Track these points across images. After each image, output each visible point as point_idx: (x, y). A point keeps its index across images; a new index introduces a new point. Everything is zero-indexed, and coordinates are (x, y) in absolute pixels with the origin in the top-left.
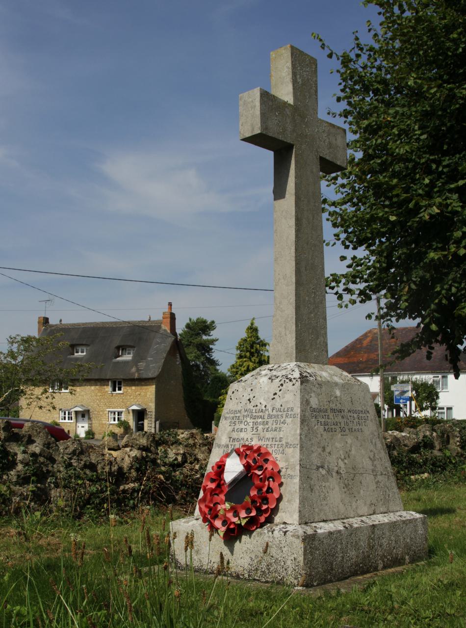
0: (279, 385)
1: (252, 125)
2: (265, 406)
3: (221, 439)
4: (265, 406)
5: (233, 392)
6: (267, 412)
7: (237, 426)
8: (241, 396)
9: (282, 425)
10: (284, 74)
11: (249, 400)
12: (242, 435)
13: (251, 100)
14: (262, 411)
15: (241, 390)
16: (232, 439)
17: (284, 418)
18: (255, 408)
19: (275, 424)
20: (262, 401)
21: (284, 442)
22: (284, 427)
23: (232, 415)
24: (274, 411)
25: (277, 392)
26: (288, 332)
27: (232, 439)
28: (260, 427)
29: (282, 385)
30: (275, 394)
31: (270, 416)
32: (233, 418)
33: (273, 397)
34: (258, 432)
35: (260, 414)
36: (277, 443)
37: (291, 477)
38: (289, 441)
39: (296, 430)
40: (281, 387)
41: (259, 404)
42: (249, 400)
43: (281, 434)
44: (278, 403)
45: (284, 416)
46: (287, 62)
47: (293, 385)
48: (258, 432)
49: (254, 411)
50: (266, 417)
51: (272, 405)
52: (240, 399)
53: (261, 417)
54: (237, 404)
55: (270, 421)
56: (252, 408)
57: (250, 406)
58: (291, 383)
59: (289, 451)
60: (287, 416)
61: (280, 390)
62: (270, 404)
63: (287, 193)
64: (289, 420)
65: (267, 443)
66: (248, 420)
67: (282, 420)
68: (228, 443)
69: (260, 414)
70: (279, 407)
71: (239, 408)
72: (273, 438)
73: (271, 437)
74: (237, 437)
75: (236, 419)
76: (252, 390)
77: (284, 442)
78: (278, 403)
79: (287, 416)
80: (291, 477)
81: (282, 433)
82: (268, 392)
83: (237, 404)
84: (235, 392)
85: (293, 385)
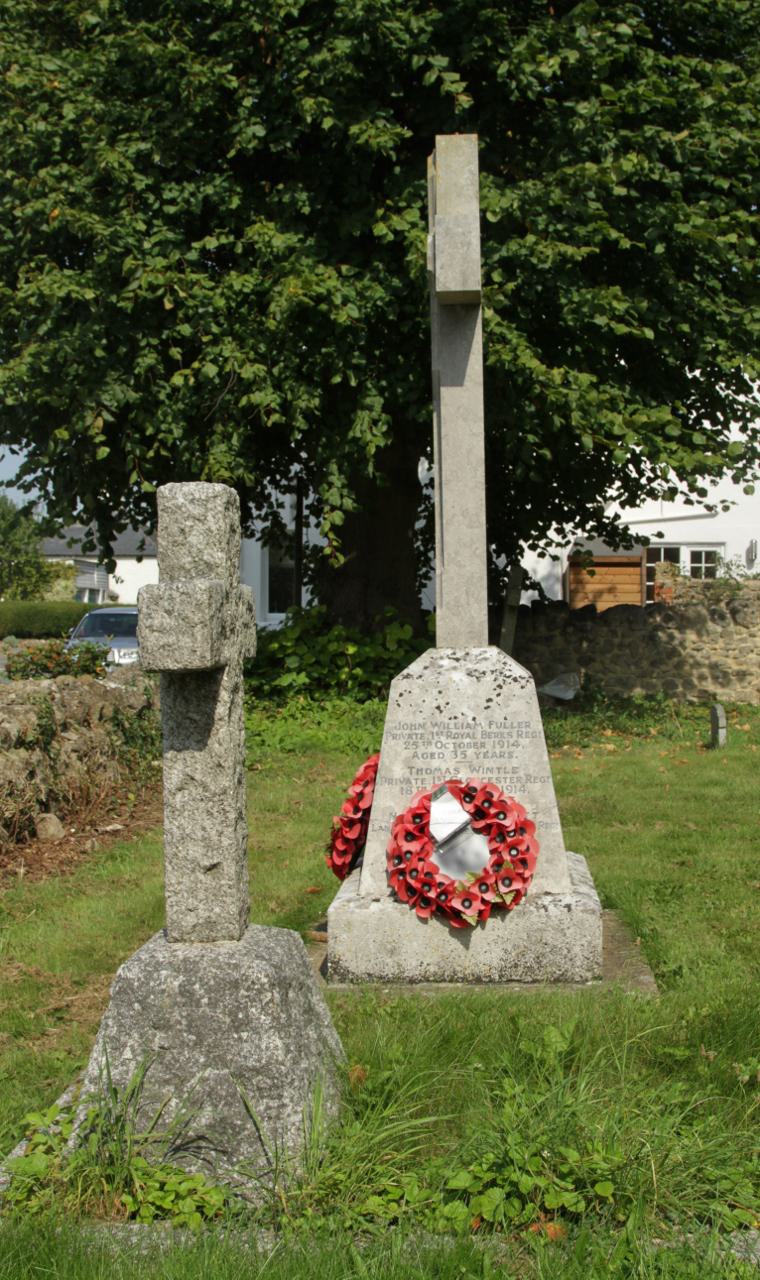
0: (494, 686)
1: (463, 273)
2: (474, 719)
3: (391, 771)
4: (474, 719)
5: (401, 695)
6: (479, 728)
7: (421, 750)
8: (420, 702)
9: (512, 749)
10: (463, 182)
11: (438, 708)
12: (435, 763)
13: (460, 230)
14: (468, 726)
15: (416, 691)
16: (414, 770)
17: (515, 738)
18: (453, 721)
19: (498, 746)
20: (465, 710)
21: (521, 774)
22: (517, 751)
23: (408, 732)
24: (493, 727)
25: (493, 697)
26: (472, 600)
27: (414, 770)
28: (470, 752)
29: (500, 687)
30: (489, 700)
31: (485, 734)
32: (410, 736)
33: (486, 705)
34: (468, 759)
35: (467, 731)
36: (508, 776)
37: (547, 825)
38: (531, 772)
39: (541, 756)
40: (498, 691)
41: (459, 715)
42: (438, 708)
43: (515, 763)
44: (498, 714)
45: (515, 735)
46: (470, 163)
47: (522, 687)
48: (468, 759)
49: (452, 726)
50: (479, 736)
51: (486, 718)
52: (417, 705)
53: (468, 735)
54: (414, 713)
55: (489, 743)
56: (446, 720)
57: (443, 718)
58: (517, 686)
59: (537, 787)
60: (519, 736)
61: (499, 695)
62: (483, 716)
63: (467, 378)
64: (524, 741)
65: (490, 775)
66: (443, 739)
67: (512, 741)
68: (407, 775)
69: (467, 731)
70: (503, 720)
71: (421, 721)
72: (499, 769)
73: (495, 766)
74: (424, 767)
75: (415, 737)
76: (440, 692)
77: (521, 774)
78: (498, 714)
79: (519, 736)
80: (547, 825)
81: (514, 760)
82: (475, 696)
83: (414, 713)
84: (405, 694)
85: (522, 687)
